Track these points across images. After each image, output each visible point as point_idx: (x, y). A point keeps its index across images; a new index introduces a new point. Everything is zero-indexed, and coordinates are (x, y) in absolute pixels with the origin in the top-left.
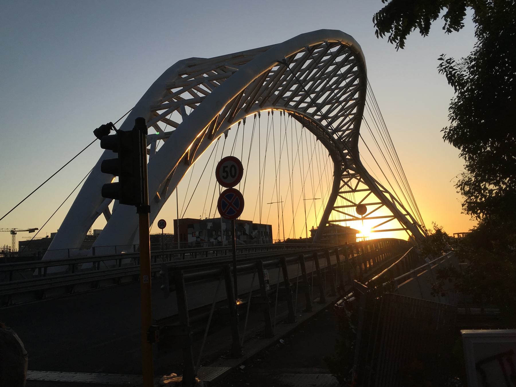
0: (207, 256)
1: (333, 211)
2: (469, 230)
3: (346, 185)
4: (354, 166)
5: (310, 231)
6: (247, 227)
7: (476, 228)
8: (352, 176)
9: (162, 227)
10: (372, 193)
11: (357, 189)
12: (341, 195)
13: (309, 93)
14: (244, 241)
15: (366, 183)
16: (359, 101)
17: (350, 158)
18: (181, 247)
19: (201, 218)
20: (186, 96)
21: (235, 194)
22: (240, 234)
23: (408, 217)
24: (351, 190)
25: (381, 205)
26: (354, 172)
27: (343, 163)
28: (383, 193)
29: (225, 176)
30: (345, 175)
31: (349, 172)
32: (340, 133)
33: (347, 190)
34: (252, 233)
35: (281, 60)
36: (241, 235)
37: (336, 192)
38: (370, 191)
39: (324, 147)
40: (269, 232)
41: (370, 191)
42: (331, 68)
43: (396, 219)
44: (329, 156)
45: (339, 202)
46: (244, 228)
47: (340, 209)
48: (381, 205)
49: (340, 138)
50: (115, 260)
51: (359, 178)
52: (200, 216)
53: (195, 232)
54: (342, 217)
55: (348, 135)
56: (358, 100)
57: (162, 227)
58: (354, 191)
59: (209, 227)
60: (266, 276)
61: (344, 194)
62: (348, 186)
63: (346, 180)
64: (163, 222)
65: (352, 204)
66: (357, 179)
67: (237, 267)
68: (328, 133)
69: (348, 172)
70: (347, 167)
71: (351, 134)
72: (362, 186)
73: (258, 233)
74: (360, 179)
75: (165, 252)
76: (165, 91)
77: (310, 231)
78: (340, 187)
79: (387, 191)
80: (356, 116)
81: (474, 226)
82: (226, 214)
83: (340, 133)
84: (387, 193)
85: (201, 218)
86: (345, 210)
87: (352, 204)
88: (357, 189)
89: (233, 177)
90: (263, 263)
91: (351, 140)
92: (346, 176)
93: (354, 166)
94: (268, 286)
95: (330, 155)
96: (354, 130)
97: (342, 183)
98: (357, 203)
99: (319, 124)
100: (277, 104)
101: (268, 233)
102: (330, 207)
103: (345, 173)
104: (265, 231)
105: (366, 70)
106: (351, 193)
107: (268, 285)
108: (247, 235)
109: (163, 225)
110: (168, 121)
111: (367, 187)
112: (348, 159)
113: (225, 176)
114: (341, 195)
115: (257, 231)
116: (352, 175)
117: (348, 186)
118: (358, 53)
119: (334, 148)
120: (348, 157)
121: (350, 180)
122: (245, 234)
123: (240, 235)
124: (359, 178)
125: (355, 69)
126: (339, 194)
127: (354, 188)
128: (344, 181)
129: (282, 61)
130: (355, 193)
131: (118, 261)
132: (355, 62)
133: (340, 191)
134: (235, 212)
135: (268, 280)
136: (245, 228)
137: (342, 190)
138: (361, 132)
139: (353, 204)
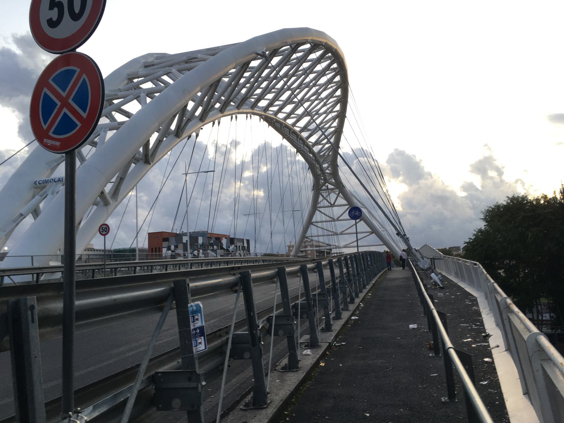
0: (166, 270)
2: (464, 243)
4: (333, 180)
5: (287, 246)
6: (224, 241)
7: (471, 241)
9: (104, 233)
12: (320, 209)
14: (221, 256)
16: (340, 113)
17: (329, 172)
18: (139, 259)
20: (148, 85)
21: (78, 70)
22: (217, 248)
26: (333, 187)
27: (322, 178)
29: (55, 19)
30: (325, 190)
31: (329, 187)
32: (320, 147)
33: (326, 205)
34: (229, 247)
36: (218, 249)
37: (315, 207)
40: (247, 247)
42: (312, 76)
44: (308, 169)
45: (318, 216)
46: (221, 242)
47: (319, 225)
49: (320, 151)
50: (31, 275)
51: (337, 193)
52: (176, 230)
53: (170, 246)
54: (320, 232)
55: (328, 148)
56: (339, 112)
57: (104, 233)
58: (332, 205)
59: (184, 241)
60: (196, 317)
62: (327, 201)
64: (106, 228)
65: (330, 219)
66: (336, 194)
67: (77, 303)
68: (308, 146)
70: (326, 181)
72: (341, 201)
73: (235, 248)
76: (127, 81)
77: (287, 246)
78: (319, 201)
80: (337, 129)
81: (469, 239)
82: (51, 133)
83: (320, 147)
86: (325, 225)
88: (335, 204)
89: (75, 17)
90: (191, 285)
91: (331, 153)
94: (200, 343)
97: (321, 198)
98: (336, 218)
100: (255, 109)
101: (246, 248)
102: (310, 222)
103: (324, 187)
104: (243, 246)
106: (330, 208)
107: (201, 340)
108: (224, 249)
109: (106, 231)
110: (127, 114)
111: (344, 202)
112: (327, 173)
113: (55, 19)
114: (320, 209)
115: (233, 246)
116: (332, 189)
119: (314, 162)
120: (327, 171)
121: (329, 194)
122: (222, 248)
123: (217, 249)
125: (338, 79)
126: (318, 209)
127: (332, 203)
128: (322, 196)
129: (262, 54)
131: (35, 276)
132: (338, 70)
134: (77, 125)
135: (201, 328)
136: (222, 242)
137: (321, 204)
138: (341, 145)
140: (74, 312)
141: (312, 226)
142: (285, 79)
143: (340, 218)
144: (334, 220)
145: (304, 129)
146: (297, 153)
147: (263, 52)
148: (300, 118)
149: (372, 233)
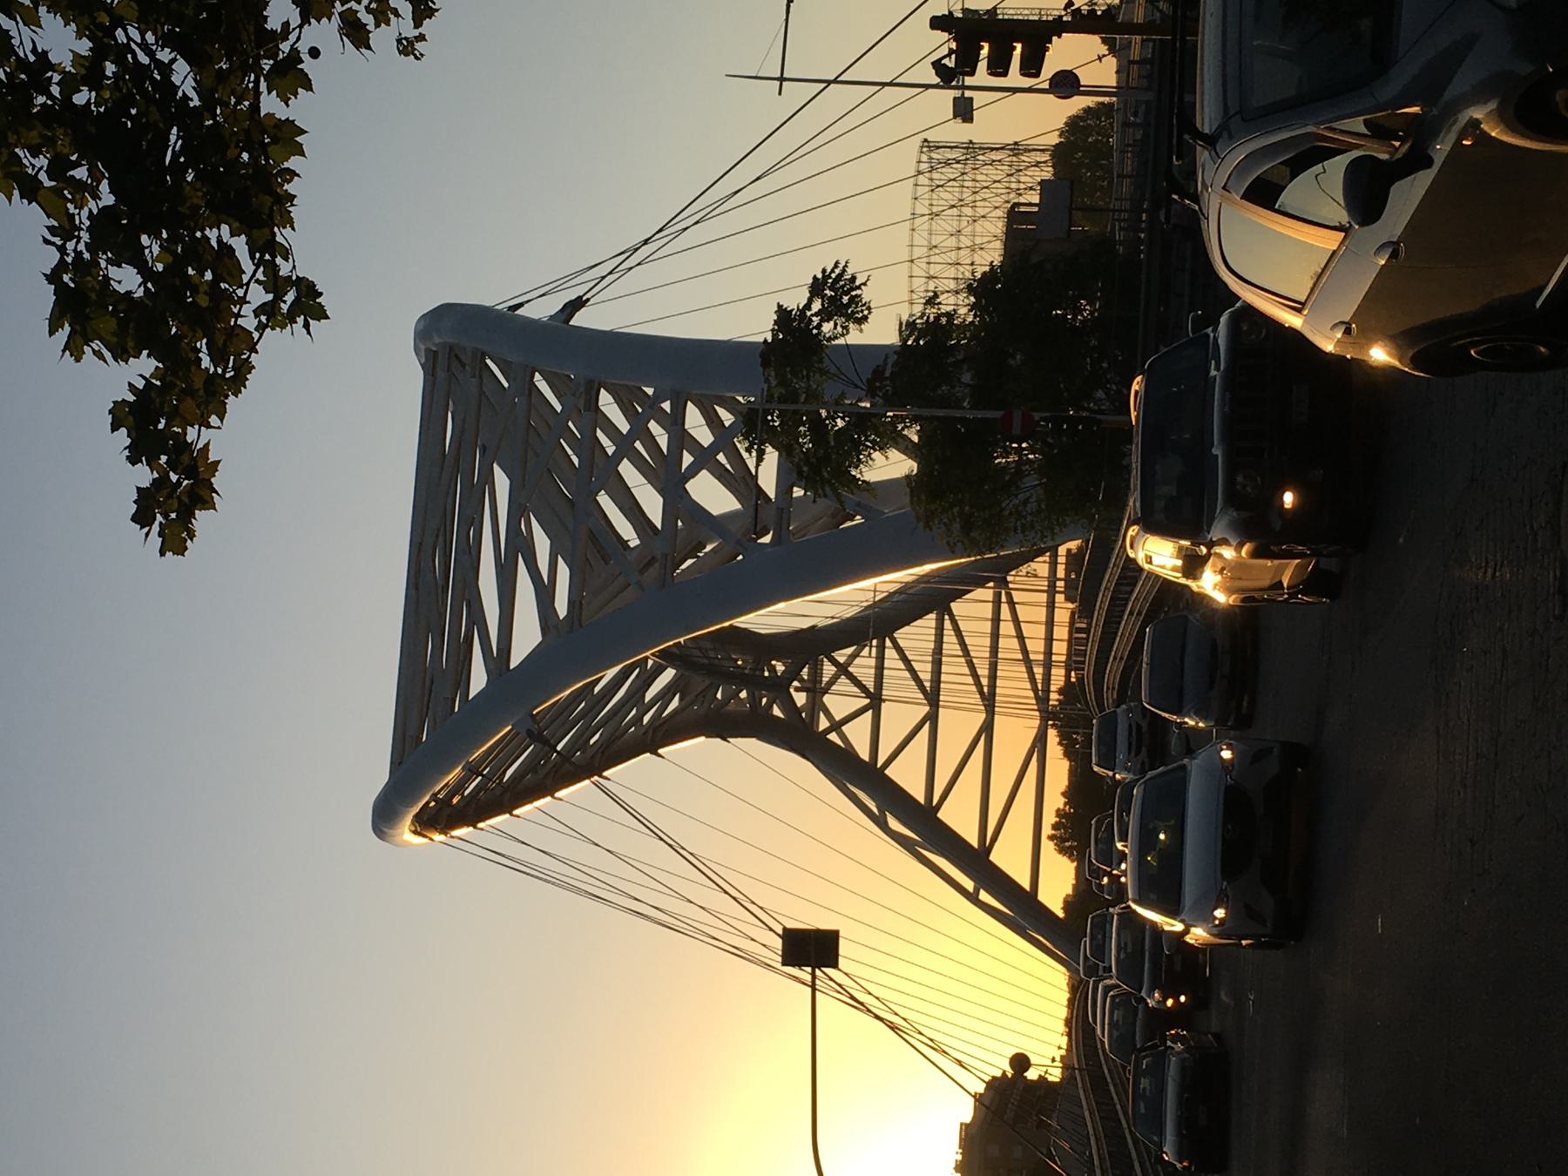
1: (940, 815)
11: (871, 686)
38: (887, 639)
41: (887, 639)
45: (908, 775)
48: (946, 617)
58: (875, 700)
63: (824, 724)
74: (834, 662)
87: (927, 726)
88: (871, 686)
92: (814, 720)
126: (879, 765)
127: (868, 701)
133: (864, 755)
139: (927, 725)
141: (940, 815)
144: (932, 718)
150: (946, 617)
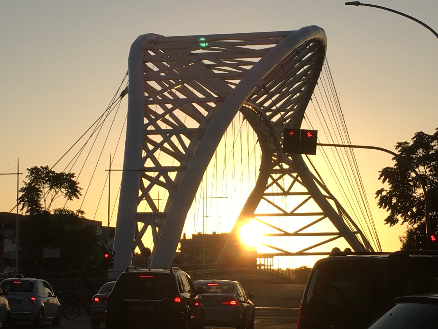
3: (275, 185)
4: (290, 158)
8: (283, 172)
10: (312, 199)
11: (291, 191)
13: (280, 110)
15: (304, 183)
19: (23, 213)
23: (358, 236)
24: (283, 192)
25: (322, 216)
27: (276, 154)
28: (327, 199)
34: (106, 243)
35: (260, 85)
38: (310, 195)
39: (251, 129)
41: (310, 195)
43: (342, 239)
44: (257, 142)
48: (322, 216)
56: (309, 77)
58: (286, 193)
61: (272, 196)
62: (280, 187)
63: (275, 176)
65: (281, 212)
66: (292, 176)
69: (281, 166)
70: (281, 159)
71: (293, 116)
72: (299, 187)
74: (297, 177)
75: (197, 272)
78: (267, 186)
79: (332, 197)
80: (304, 95)
84: (332, 199)
85: (23, 213)
87: (281, 212)
88: (291, 191)
92: (276, 172)
93: (290, 158)
95: (258, 142)
96: (297, 112)
97: (270, 181)
99: (259, 111)
103: (277, 167)
105: (325, 50)
106: (283, 196)
111: (305, 190)
117: (280, 187)
118: (322, 40)
124: (295, 175)
126: (264, 197)
127: (286, 190)
130: (288, 196)
133: (266, 192)
139: (283, 213)
140: (190, 298)
142: (282, 113)
143: (295, 212)
144: (286, 214)
145: (269, 109)
146: (244, 120)
147: (263, 85)
148: (275, 113)
149: (340, 235)
150: (323, 216)
